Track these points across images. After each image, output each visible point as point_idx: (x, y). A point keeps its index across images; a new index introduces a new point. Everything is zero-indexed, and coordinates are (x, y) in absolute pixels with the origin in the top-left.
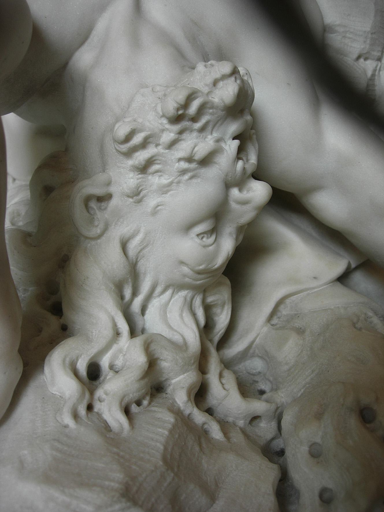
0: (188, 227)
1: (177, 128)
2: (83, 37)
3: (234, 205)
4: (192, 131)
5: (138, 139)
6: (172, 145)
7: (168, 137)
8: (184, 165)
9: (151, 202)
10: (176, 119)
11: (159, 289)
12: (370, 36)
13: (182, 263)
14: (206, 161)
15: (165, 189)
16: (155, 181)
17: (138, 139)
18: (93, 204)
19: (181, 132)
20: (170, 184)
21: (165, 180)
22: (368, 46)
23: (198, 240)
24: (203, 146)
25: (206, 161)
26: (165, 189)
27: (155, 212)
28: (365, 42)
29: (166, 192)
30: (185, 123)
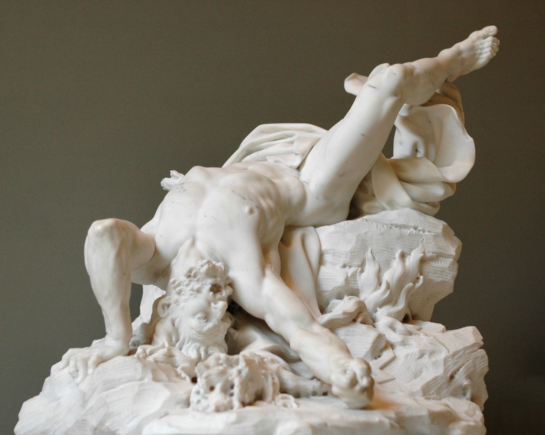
0: (194, 315)
1: (189, 279)
2: (175, 255)
3: (213, 310)
4: (194, 281)
5: (177, 283)
6: (188, 285)
7: (187, 282)
8: (191, 292)
9: (182, 305)
10: (189, 276)
11: (186, 341)
12: (349, 253)
13: (192, 328)
14: (199, 291)
15: (186, 300)
16: (183, 298)
17: (177, 283)
18: (166, 308)
19: (190, 281)
20: (187, 298)
21: (186, 297)
22: (349, 259)
23: (197, 320)
24: (196, 286)
25: (199, 291)
26: (186, 300)
27: (183, 309)
28: (346, 257)
29: (186, 302)
30: (192, 278)
